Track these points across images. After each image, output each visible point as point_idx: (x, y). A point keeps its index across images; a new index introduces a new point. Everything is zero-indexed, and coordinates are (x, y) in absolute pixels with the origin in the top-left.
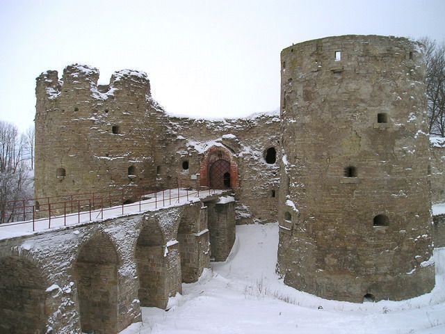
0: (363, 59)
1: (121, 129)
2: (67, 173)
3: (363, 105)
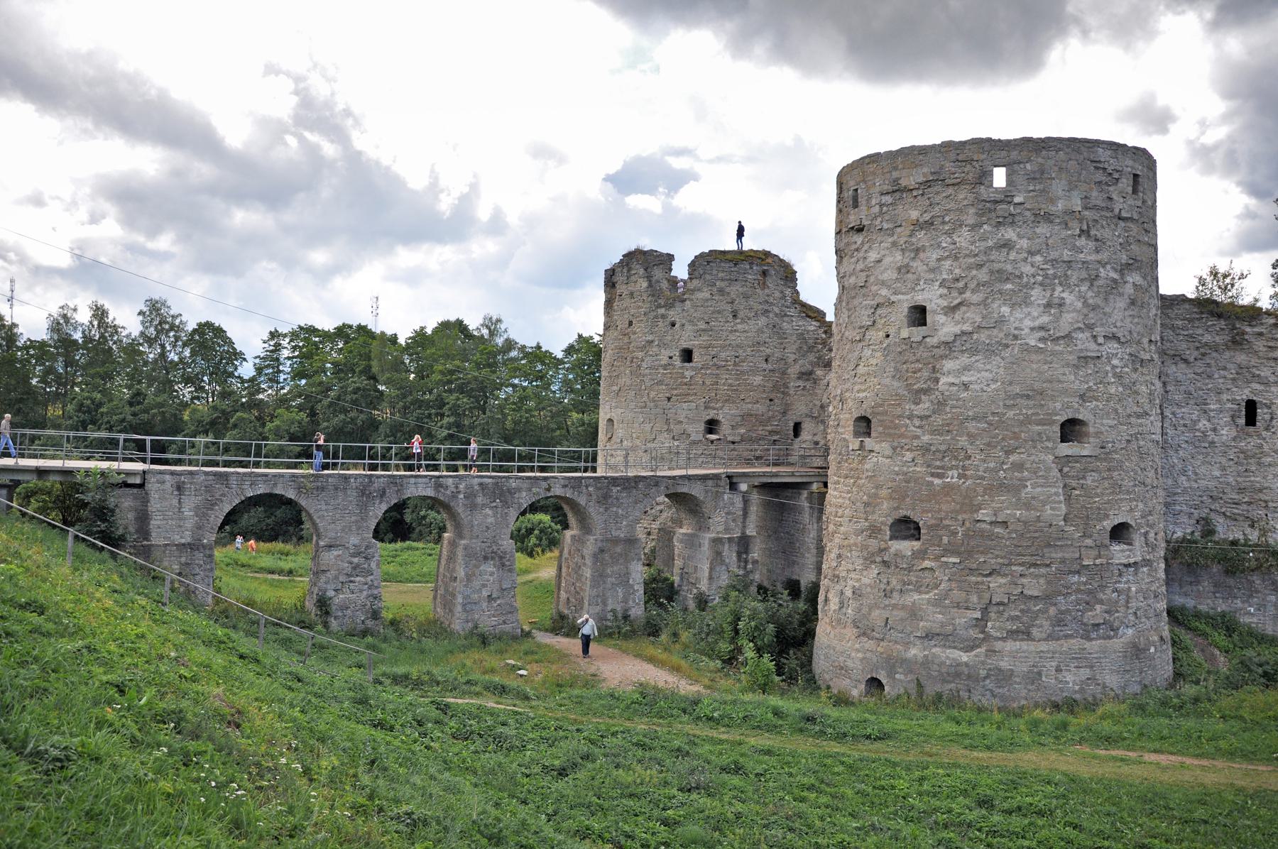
0: (888, 199)
3: (884, 292)
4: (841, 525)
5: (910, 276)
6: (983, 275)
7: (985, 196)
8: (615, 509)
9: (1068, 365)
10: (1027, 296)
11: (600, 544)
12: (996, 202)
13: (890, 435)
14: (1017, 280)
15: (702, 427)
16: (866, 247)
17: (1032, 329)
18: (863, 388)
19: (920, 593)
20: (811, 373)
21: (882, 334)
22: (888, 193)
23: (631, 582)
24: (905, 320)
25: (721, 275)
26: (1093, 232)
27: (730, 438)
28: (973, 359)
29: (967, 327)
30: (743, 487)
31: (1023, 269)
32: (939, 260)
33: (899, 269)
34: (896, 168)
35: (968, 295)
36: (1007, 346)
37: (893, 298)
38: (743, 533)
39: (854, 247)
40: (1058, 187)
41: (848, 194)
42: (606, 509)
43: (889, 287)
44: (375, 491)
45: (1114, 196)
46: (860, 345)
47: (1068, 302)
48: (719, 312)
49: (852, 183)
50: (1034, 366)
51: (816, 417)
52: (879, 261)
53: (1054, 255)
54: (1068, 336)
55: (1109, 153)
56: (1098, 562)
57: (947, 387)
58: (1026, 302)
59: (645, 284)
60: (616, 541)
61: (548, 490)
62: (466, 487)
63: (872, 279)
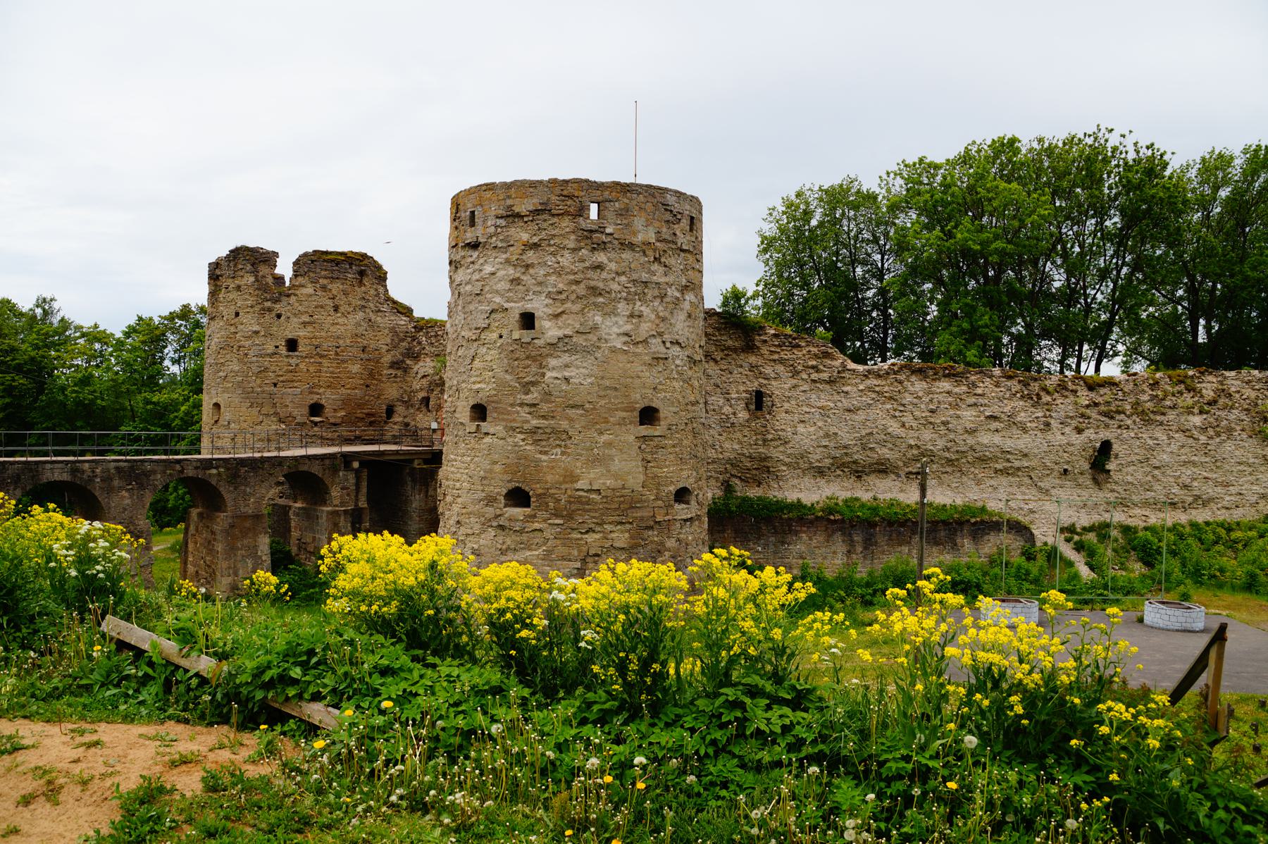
0: (502, 222)
1: (301, 342)
2: (222, 410)
3: (498, 299)
4: (459, 497)
5: (520, 287)
6: (581, 290)
7: (584, 226)
8: (243, 488)
9: (645, 364)
10: (615, 308)
11: (230, 521)
12: (591, 231)
13: (503, 420)
14: (607, 295)
15: (306, 411)
16: (481, 261)
17: (618, 335)
18: (479, 379)
19: (530, 550)
20: (403, 361)
21: (495, 336)
22: (502, 217)
23: (259, 553)
24: (517, 325)
25: (323, 273)
26: (663, 260)
27: (332, 420)
28: (573, 358)
29: (568, 332)
30: (356, 465)
31: (612, 287)
32: (545, 275)
33: (512, 281)
34: (509, 197)
35: (569, 305)
36: (599, 348)
37: (506, 305)
38: (356, 505)
39: (470, 260)
40: (639, 222)
41: (465, 215)
42: (235, 489)
43: (502, 296)
44: (9, 478)
45: (678, 233)
46: (476, 344)
47: (645, 314)
48: (322, 307)
49: (469, 205)
50: (621, 365)
51: (406, 402)
52: (493, 274)
53: (635, 276)
54: (645, 341)
55: (674, 198)
56: (666, 518)
57: (552, 380)
58: (614, 313)
59: (252, 279)
60: (245, 517)
61: (182, 472)
62: (103, 472)
63: (487, 288)
